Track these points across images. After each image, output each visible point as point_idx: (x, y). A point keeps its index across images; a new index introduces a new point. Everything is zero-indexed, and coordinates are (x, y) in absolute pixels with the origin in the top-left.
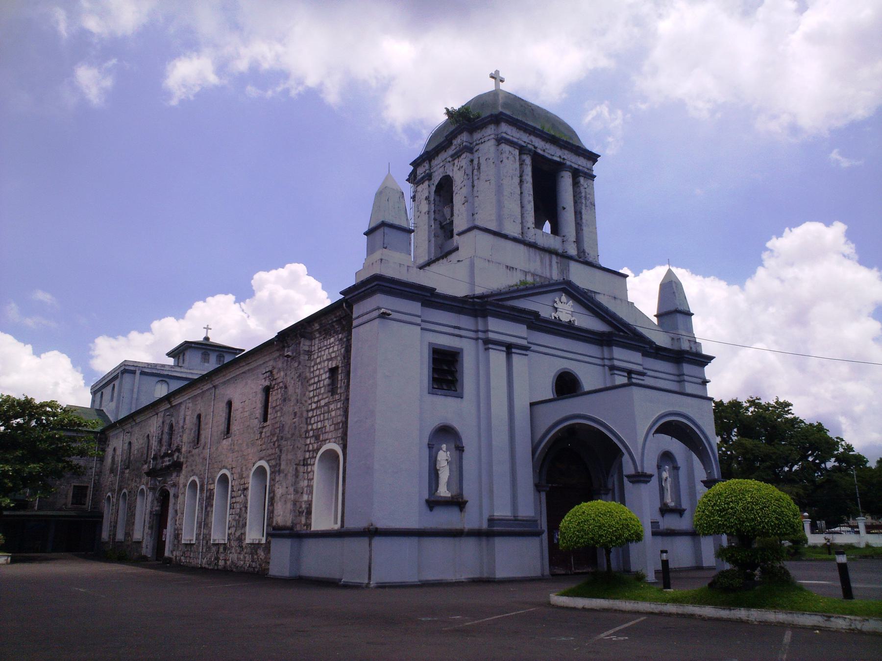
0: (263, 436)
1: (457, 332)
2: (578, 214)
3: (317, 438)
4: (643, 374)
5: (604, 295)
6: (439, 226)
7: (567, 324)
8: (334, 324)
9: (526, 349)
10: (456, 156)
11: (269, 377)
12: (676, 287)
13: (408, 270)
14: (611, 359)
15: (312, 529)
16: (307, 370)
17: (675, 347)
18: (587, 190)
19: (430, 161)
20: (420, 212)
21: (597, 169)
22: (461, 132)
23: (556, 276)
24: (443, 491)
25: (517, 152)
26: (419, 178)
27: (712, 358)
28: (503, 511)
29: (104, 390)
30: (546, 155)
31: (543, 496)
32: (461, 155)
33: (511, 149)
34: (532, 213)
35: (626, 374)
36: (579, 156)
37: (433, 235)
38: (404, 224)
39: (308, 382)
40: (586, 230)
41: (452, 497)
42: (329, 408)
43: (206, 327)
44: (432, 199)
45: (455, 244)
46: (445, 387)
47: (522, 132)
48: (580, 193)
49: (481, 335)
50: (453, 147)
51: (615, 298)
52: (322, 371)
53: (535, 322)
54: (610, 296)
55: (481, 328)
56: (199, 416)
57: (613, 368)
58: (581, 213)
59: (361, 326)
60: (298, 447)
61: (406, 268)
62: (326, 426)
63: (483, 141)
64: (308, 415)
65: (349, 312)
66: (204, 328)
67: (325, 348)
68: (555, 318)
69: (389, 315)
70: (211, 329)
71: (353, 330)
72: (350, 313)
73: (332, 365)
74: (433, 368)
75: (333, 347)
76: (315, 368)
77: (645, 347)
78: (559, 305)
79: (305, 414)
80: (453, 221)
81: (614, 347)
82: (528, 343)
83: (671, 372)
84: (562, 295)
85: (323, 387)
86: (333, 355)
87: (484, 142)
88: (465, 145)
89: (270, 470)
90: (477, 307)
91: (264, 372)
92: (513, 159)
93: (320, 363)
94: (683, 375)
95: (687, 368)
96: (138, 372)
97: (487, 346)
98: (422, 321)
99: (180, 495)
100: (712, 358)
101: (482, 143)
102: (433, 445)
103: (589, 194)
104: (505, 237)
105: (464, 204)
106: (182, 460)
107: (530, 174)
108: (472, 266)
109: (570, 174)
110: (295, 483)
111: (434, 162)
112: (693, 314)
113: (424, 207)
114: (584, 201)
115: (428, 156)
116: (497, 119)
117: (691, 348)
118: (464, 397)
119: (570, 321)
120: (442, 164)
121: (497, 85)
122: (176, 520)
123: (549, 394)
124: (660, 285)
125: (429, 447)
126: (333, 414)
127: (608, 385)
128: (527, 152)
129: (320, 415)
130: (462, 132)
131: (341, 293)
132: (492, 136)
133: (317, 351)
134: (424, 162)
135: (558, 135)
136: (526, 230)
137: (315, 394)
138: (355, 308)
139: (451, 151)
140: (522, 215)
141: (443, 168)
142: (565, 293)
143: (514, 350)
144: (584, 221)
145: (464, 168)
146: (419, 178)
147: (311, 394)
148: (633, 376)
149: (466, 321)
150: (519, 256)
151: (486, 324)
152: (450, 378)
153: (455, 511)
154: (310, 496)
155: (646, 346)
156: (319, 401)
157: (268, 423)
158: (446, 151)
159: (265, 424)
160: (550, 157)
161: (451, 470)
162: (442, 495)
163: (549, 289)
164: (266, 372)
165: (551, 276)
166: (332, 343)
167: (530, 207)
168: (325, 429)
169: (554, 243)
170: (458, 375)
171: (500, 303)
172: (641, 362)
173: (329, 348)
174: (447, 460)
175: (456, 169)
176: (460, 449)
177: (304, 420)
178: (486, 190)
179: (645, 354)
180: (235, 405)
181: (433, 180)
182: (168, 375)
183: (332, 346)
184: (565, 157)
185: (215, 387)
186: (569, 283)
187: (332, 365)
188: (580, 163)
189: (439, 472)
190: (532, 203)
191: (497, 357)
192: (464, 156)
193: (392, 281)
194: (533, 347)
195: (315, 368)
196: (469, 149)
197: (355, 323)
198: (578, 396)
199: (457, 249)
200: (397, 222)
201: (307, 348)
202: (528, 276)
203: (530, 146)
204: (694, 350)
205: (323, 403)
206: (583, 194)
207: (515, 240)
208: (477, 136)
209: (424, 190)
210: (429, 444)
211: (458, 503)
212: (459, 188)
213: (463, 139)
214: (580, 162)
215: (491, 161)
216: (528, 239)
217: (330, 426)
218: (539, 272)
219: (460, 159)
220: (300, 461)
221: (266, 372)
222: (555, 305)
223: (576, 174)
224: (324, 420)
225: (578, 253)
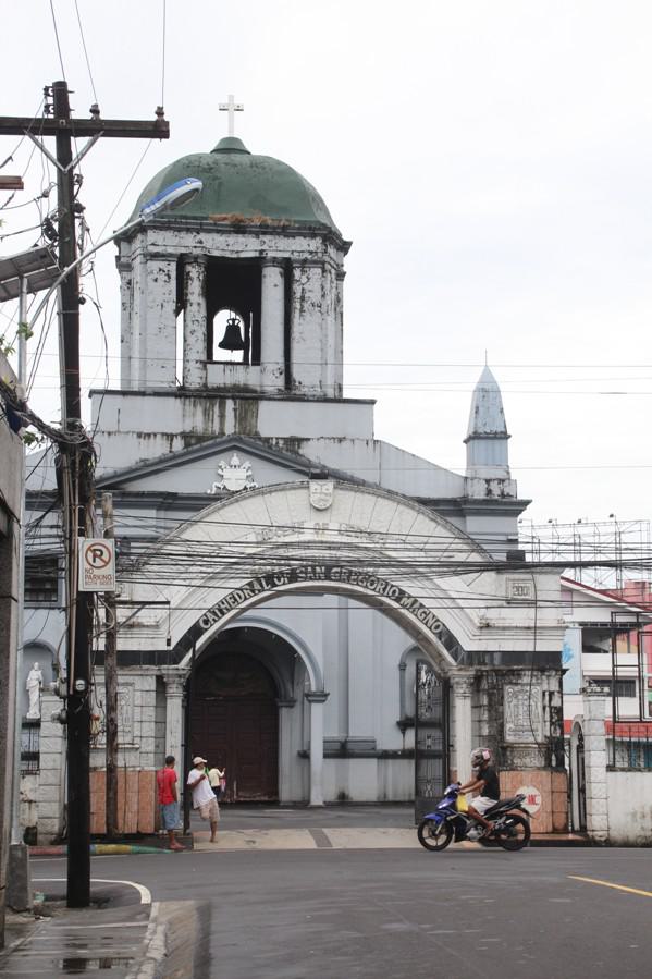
30: (228, 255)
33: (162, 265)
36: (294, 237)
47: (183, 234)
78: (227, 473)
103: (310, 291)
112: (510, 436)
114: (298, 305)
117: (489, 492)
152: (48, 586)
160: (235, 256)
188: (293, 248)
206: (298, 295)
222: (220, 471)
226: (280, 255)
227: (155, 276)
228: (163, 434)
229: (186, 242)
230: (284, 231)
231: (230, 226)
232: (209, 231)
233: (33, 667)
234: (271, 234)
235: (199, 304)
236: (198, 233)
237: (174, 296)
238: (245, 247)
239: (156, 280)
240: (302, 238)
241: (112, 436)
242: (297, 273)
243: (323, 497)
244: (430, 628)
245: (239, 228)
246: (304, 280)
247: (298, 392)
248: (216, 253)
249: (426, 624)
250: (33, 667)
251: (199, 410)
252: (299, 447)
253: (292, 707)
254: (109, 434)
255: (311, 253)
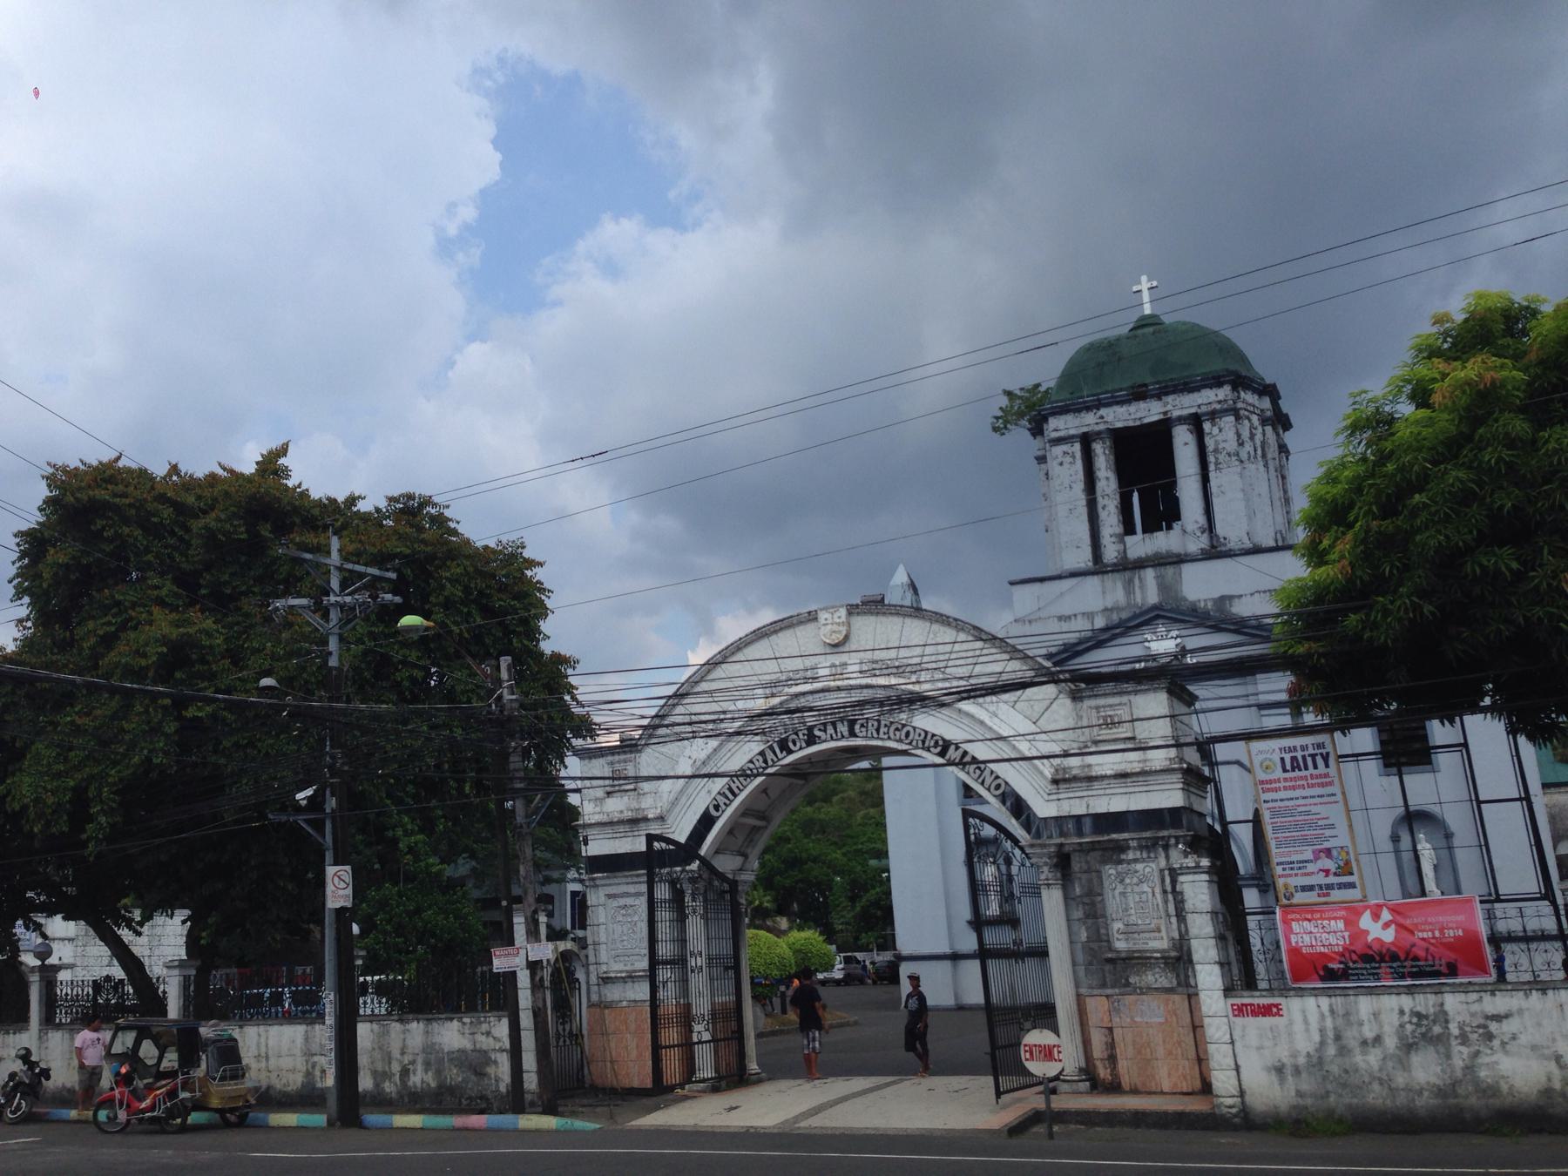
18: (1219, 438)
30: (1131, 424)
33: (1065, 448)
36: (1199, 391)
103: (1225, 441)
160: (1138, 423)
184: (1169, 407)
188: (1200, 402)
202: (1096, 618)
203: (1097, 428)
226: (1185, 412)
227: (1059, 460)
228: (1084, 614)
229: (1088, 421)
230: (1188, 387)
231: (1128, 395)
234: (1174, 392)
235: (1107, 478)
236: (1098, 409)
237: (1081, 475)
238: (1149, 412)
239: (1061, 464)
240: (1208, 390)
241: (1034, 624)
242: (1207, 426)
243: (835, 628)
244: (989, 789)
245: (1139, 394)
246: (1215, 430)
247: (1223, 549)
248: (1119, 425)
249: (982, 783)
251: (1119, 585)
252: (1231, 606)
255: (1220, 402)
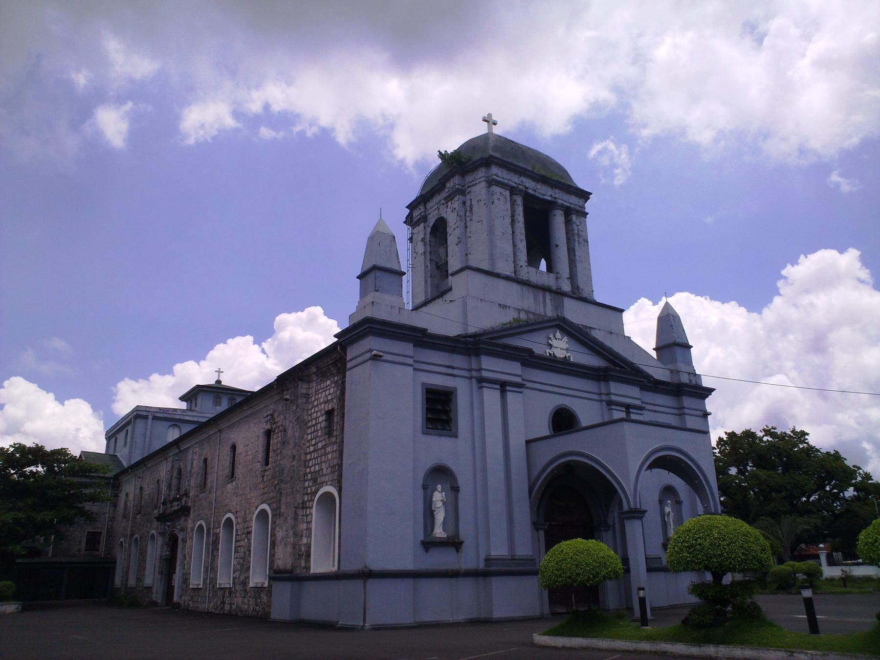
0: (265, 480)
1: (450, 371)
2: (571, 251)
3: (315, 480)
4: (641, 408)
5: (600, 330)
6: (435, 266)
7: (561, 360)
8: (330, 366)
9: (520, 386)
10: (449, 198)
11: (270, 420)
12: (674, 320)
13: (399, 311)
14: (609, 394)
15: (311, 572)
16: (305, 412)
17: (675, 381)
18: (580, 228)
19: (425, 204)
20: (417, 254)
21: (589, 206)
22: (453, 176)
23: (550, 312)
24: (439, 532)
25: (508, 193)
26: (414, 220)
27: (713, 390)
28: (499, 550)
29: (118, 436)
30: (537, 194)
31: (542, 533)
32: (454, 197)
33: (502, 190)
34: (525, 251)
35: (624, 409)
37: (429, 275)
38: (395, 267)
39: (306, 424)
40: (579, 267)
41: (448, 537)
42: (325, 450)
43: (218, 370)
44: (428, 240)
45: (450, 284)
46: (439, 427)
47: (512, 174)
48: (573, 230)
49: (474, 374)
50: (447, 190)
51: (611, 333)
52: (319, 414)
53: (529, 359)
54: (606, 331)
55: (474, 366)
56: (206, 460)
57: (610, 403)
58: (574, 250)
59: (354, 369)
60: (296, 490)
61: (398, 310)
62: (323, 469)
63: (474, 183)
64: (306, 457)
65: (344, 355)
66: (216, 371)
67: (321, 391)
68: (550, 354)
69: (381, 356)
70: (222, 372)
71: (347, 372)
72: (344, 355)
73: (328, 408)
74: (427, 408)
75: (329, 389)
76: (313, 411)
77: (643, 382)
78: (554, 342)
79: (303, 457)
80: (447, 261)
81: (610, 382)
82: (523, 380)
83: (670, 405)
84: (557, 332)
85: (320, 430)
86: (330, 397)
87: (476, 184)
88: (458, 188)
89: (272, 513)
90: (469, 346)
91: (266, 415)
92: (504, 199)
93: (317, 406)
94: (684, 408)
95: (687, 401)
96: (150, 417)
97: (480, 385)
98: (414, 361)
99: (188, 539)
100: (713, 390)
101: (474, 186)
102: (428, 486)
104: (498, 276)
105: (457, 245)
106: (190, 504)
107: (522, 214)
108: (465, 305)
109: (562, 212)
110: (295, 526)
111: (429, 205)
112: (692, 347)
113: (421, 248)
115: (422, 200)
116: (487, 162)
117: (690, 381)
118: (459, 436)
119: (566, 357)
120: (436, 207)
121: (490, 128)
122: (185, 565)
123: (545, 431)
124: (658, 318)
125: (424, 488)
126: (330, 456)
127: (606, 420)
128: (518, 193)
129: (317, 457)
130: (455, 176)
131: (335, 336)
132: (483, 179)
133: (314, 394)
134: (419, 205)
135: (548, 175)
136: (518, 268)
137: (313, 437)
138: (349, 350)
139: (444, 194)
140: (515, 253)
141: (437, 210)
142: (560, 329)
143: (508, 388)
144: (577, 257)
145: (456, 210)
146: (414, 220)
147: (309, 437)
148: (631, 410)
149: (459, 361)
150: (512, 295)
151: (479, 362)
152: (444, 417)
153: (452, 551)
154: (309, 539)
155: (644, 380)
156: (316, 444)
157: (270, 466)
158: (440, 194)
159: (267, 468)
160: (541, 196)
161: (446, 511)
162: (437, 536)
163: (540, 326)
164: (267, 416)
165: (545, 312)
166: (329, 385)
167: (522, 246)
168: (322, 472)
169: (549, 280)
170: (452, 415)
171: (493, 341)
172: (638, 397)
173: (326, 390)
174: (442, 500)
175: (449, 210)
176: (455, 489)
177: (302, 463)
178: (478, 230)
179: (643, 388)
180: (240, 449)
181: (428, 221)
182: (179, 419)
183: (328, 388)
184: (556, 196)
185: (220, 431)
186: (564, 320)
187: (328, 408)
188: (571, 201)
189: (435, 513)
190: (524, 242)
191: (492, 396)
192: (456, 198)
193: (384, 323)
194: (528, 384)
195: (313, 411)
196: (462, 192)
197: (349, 365)
198: (577, 431)
199: (450, 289)
200: (388, 265)
201: (304, 391)
203: (520, 187)
204: (694, 382)
205: (320, 445)
206: (576, 232)
207: (507, 278)
208: (469, 178)
209: (421, 231)
210: (423, 485)
211: (454, 543)
212: (452, 230)
213: (455, 182)
214: (573, 201)
215: (483, 202)
216: (521, 277)
217: (327, 468)
218: (532, 309)
219: (453, 202)
220: (299, 504)
221: (267, 416)
222: (550, 341)
223: (568, 212)
224: (321, 463)
225: (572, 289)
228: (514, 308)
232: (527, 176)
233: (436, 490)
250: (436, 490)
253: (607, 531)
254: (481, 300)
